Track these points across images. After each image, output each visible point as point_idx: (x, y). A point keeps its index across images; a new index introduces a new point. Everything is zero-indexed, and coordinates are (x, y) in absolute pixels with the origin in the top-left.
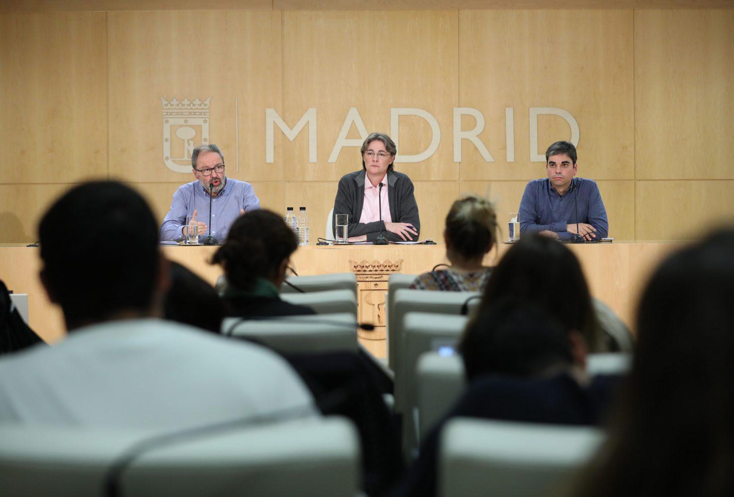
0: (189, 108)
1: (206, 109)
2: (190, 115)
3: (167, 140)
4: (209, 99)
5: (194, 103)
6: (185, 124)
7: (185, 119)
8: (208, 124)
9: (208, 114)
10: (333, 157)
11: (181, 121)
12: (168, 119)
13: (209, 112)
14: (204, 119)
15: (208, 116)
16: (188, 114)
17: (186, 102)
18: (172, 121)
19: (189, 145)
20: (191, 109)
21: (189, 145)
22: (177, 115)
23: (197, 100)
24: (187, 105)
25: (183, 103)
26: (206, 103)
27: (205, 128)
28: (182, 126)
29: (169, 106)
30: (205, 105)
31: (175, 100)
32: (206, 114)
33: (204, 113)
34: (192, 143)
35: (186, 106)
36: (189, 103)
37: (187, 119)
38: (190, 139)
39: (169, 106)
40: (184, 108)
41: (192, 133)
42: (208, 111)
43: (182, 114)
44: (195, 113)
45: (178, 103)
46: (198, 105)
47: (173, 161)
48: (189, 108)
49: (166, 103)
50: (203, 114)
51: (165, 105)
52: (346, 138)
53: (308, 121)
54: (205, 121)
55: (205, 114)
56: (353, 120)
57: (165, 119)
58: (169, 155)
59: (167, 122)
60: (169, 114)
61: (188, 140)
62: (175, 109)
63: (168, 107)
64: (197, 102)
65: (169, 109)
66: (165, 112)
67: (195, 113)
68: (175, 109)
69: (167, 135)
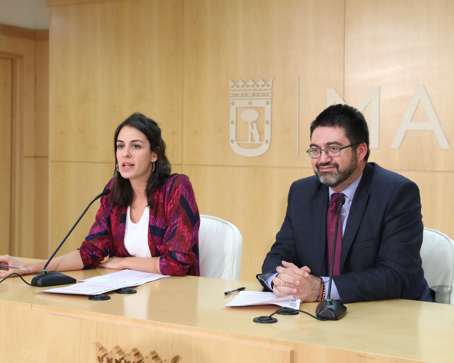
0: (253, 89)
1: (269, 90)
2: (254, 96)
3: (232, 122)
4: (272, 79)
5: (258, 83)
6: (249, 106)
7: (249, 101)
8: (270, 106)
9: (271, 95)
10: (395, 145)
11: (246, 103)
12: (234, 101)
13: (272, 93)
14: (267, 100)
15: (271, 97)
16: (252, 95)
17: (251, 83)
18: (238, 103)
19: (253, 128)
20: (255, 90)
21: (253, 128)
22: (242, 96)
23: (261, 80)
24: (252, 86)
25: (248, 84)
26: (268, 83)
27: (268, 108)
28: (246, 108)
29: (235, 88)
30: (268, 86)
31: (241, 81)
32: (269, 95)
33: (267, 94)
34: (255, 125)
35: (250, 87)
36: (253, 83)
37: (252, 101)
38: (254, 122)
39: (235, 88)
40: (248, 89)
41: (254, 115)
42: (271, 92)
43: (246, 95)
44: (258, 95)
45: (243, 84)
46: (262, 86)
47: (238, 144)
48: (253, 89)
49: (233, 84)
50: (266, 95)
51: (232, 86)
52: (411, 121)
53: (370, 101)
54: (267, 103)
55: (267, 95)
56: (420, 100)
57: (231, 101)
58: (234, 139)
59: (233, 103)
60: (235, 95)
61: (252, 123)
62: (240, 90)
63: (233, 89)
64: (261, 83)
65: (235, 90)
66: (232, 94)
67: (258, 95)
68: (240, 90)
69: (233, 117)
